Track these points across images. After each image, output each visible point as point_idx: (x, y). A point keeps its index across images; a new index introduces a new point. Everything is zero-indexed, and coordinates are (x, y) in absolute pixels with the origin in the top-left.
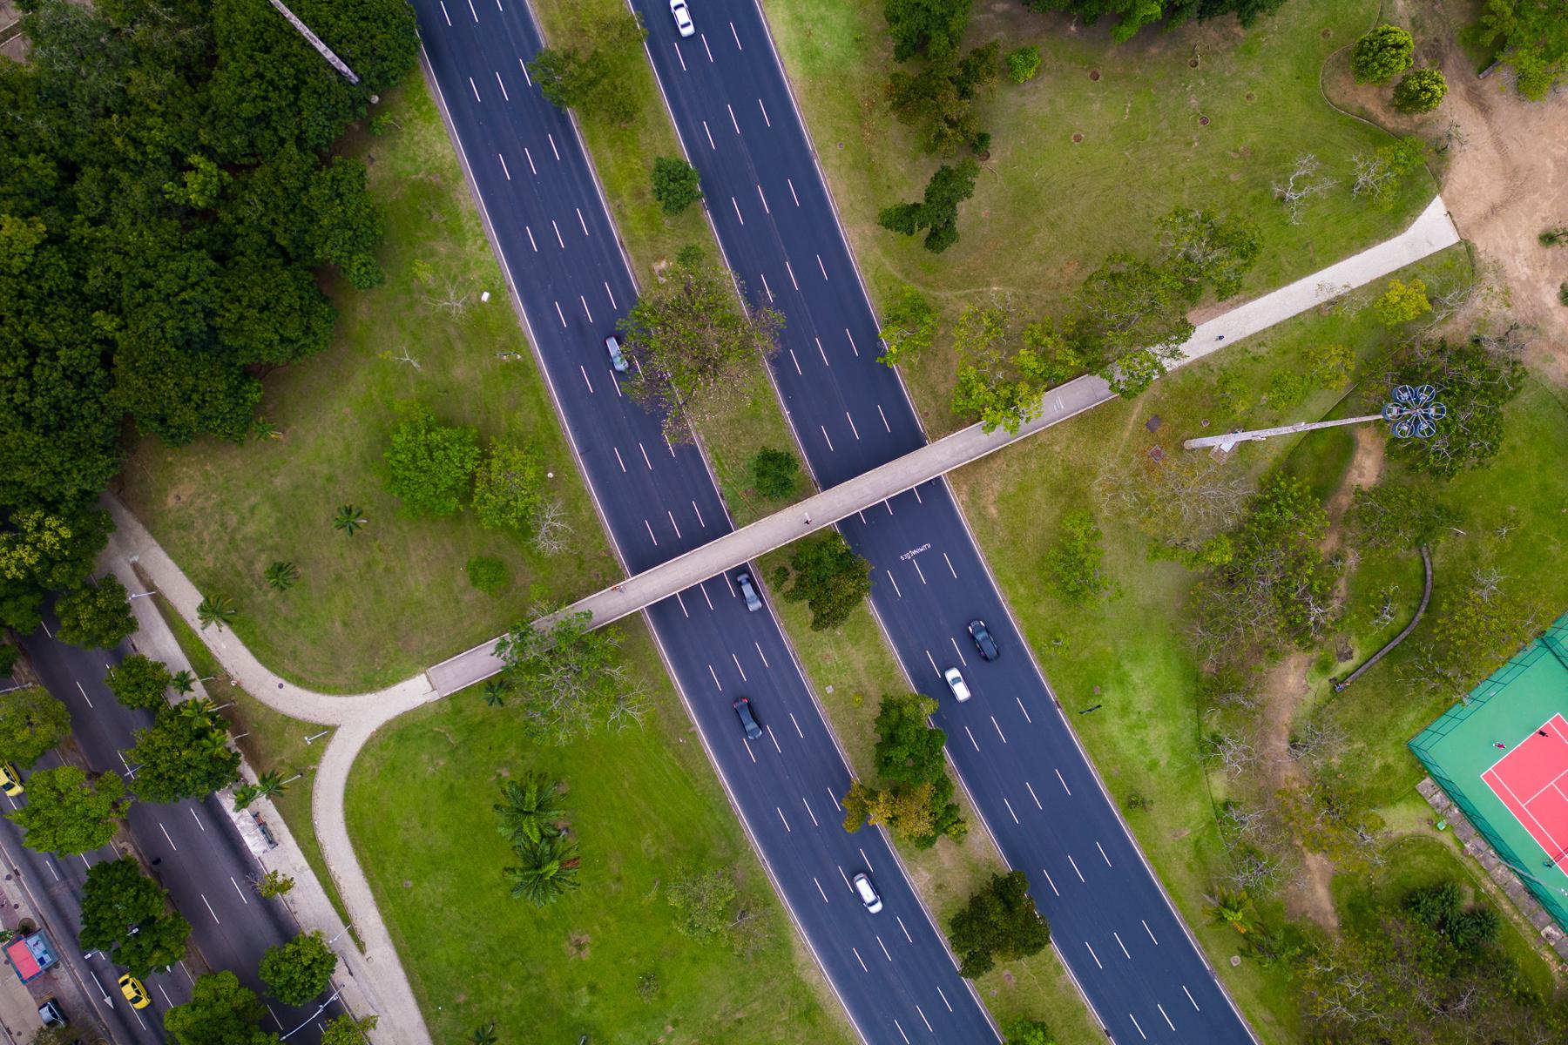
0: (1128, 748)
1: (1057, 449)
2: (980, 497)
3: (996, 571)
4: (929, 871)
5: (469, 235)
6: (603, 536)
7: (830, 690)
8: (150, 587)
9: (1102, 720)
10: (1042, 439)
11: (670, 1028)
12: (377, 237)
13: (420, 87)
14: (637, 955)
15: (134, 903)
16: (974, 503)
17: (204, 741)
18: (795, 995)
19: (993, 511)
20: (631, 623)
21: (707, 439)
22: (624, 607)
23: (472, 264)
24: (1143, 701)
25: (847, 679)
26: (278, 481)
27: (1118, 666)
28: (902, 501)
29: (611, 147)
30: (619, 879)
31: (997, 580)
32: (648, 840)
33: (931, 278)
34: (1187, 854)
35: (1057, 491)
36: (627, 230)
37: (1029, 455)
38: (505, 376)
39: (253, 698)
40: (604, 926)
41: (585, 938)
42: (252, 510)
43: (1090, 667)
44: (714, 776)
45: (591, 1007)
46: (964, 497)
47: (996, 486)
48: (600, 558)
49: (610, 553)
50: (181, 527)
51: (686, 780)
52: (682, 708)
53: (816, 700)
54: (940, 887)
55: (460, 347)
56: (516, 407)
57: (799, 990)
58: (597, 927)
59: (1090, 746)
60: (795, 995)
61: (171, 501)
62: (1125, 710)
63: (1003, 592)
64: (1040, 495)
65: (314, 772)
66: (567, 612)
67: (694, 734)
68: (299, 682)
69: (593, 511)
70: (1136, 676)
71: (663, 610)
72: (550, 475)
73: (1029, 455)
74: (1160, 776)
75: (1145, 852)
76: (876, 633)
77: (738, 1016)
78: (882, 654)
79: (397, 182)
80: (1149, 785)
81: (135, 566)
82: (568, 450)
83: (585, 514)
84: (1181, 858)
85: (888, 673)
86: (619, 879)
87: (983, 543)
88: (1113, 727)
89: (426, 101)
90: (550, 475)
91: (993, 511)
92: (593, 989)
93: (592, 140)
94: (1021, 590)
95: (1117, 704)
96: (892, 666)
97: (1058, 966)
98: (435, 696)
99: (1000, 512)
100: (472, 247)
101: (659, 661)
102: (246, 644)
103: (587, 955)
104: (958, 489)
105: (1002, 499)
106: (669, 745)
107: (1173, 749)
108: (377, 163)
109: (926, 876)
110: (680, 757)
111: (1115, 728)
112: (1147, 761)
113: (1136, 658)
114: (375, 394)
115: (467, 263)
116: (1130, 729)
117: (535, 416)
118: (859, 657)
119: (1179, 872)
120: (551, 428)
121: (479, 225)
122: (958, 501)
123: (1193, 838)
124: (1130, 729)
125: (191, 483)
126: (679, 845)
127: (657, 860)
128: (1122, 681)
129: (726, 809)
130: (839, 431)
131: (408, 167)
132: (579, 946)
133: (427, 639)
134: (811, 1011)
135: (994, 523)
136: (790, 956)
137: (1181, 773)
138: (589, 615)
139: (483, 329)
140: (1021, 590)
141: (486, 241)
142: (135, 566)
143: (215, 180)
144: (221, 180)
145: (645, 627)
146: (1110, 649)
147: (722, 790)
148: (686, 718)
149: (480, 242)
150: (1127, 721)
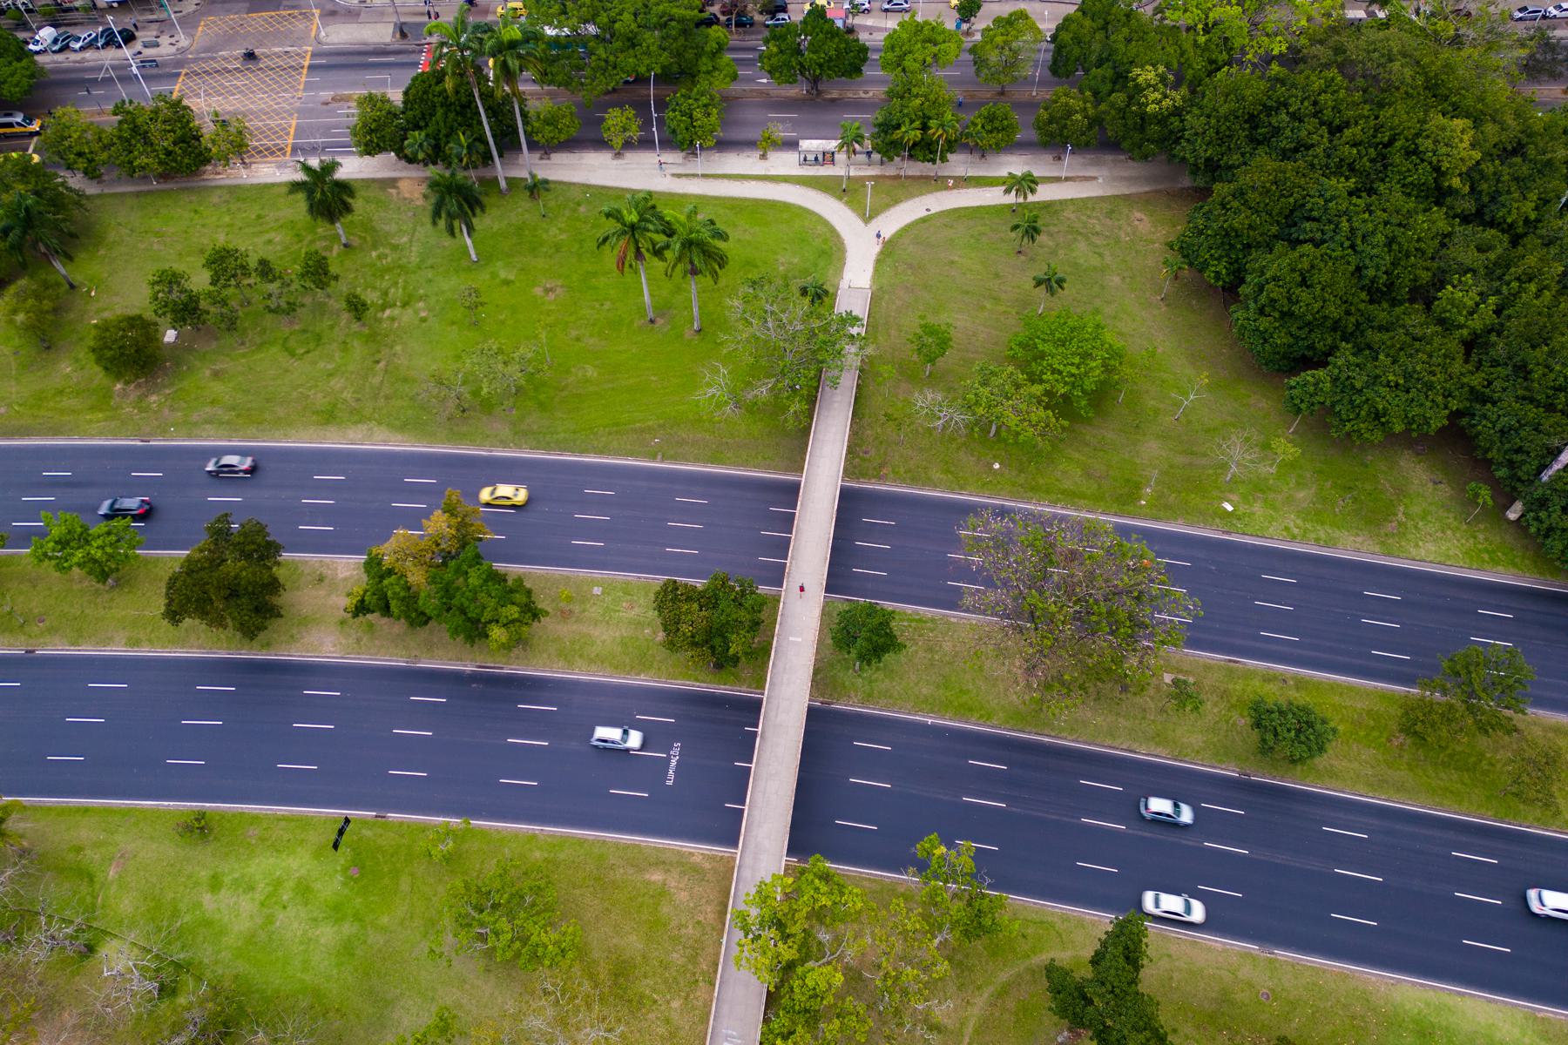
0: (262, 866)
1: (675, 1004)
2: (683, 873)
3: (582, 842)
4: (345, 579)
5: (1309, 526)
6: (903, 480)
7: (597, 590)
8: (1067, 179)
9: (317, 854)
10: (701, 993)
11: (423, 314)
12: (1341, 429)
13: (1514, 565)
14: (503, 322)
15: (823, 66)
16: (680, 864)
17: (917, 124)
18: (353, 411)
19: (657, 877)
20: (797, 442)
21: (948, 623)
22: (820, 436)
23: (1270, 498)
24: (292, 922)
25: (594, 611)
26: (1117, 279)
27: (358, 918)
28: (739, 785)
29: (1369, 712)
30: (578, 339)
31: (573, 837)
32: (591, 372)
33: (1011, 1004)
34: (92, 856)
35: (622, 971)
36: (1249, 674)
37: (693, 959)
38: (1128, 481)
39: (931, 192)
40: (549, 313)
41: (552, 296)
42: (1100, 255)
43: (386, 881)
44: (600, 452)
45: (494, 276)
46: (697, 859)
47: (684, 896)
48: (882, 466)
49: (882, 479)
50: (1112, 211)
51: (617, 424)
52: (684, 459)
53: (597, 574)
54: (321, 579)
55: (1180, 460)
56: (1088, 474)
57: (357, 416)
58: (553, 307)
59: (305, 822)
60: (353, 411)
61: (1138, 215)
62: (304, 890)
63: (553, 835)
64: (633, 943)
65: (840, 199)
66: (848, 382)
67: (653, 458)
68: (923, 220)
69: (935, 486)
70: (327, 934)
71: (791, 492)
72: (997, 466)
73: (693, 959)
74: (197, 884)
75: (143, 811)
76: (618, 667)
77: (382, 364)
78: (591, 661)
79: (1401, 492)
80: (203, 864)
81: (1095, 178)
82: (1013, 497)
83: (936, 475)
84: (97, 845)
86: (578, 339)
87: (627, 847)
88: (299, 863)
89: (1495, 562)
90: (997, 466)
91: (657, 877)
92: (507, 283)
93: (1383, 696)
94: (538, 854)
95: (318, 886)
96: (570, 664)
97: (136, 643)
98: (844, 284)
99: (649, 883)
100: (1293, 521)
101: (745, 464)
102: (979, 207)
103: (538, 291)
104: (713, 858)
105: (662, 893)
106: (660, 426)
107: (208, 923)
108: (1430, 485)
109: (342, 573)
110: (642, 431)
111: (295, 866)
112: (227, 880)
113: (347, 949)
114: (1165, 376)
115: (1275, 508)
116: (278, 884)
117: (1067, 484)
118: (605, 637)
119: (85, 832)
120: (1048, 492)
121: (1317, 540)
122: (698, 850)
123: (99, 877)
124: (278, 884)
125: (1151, 232)
126: (565, 393)
127: (568, 372)
128: (337, 912)
129: (562, 447)
130: (872, 765)
131: (1415, 510)
132: (548, 291)
133: (898, 303)
134: (329, 417)
135: (641, 870)
136: (390, 426)
137: (175, 914)
138: (835, 385)
139: (1193, 482)
140: (538, 854)
141: (1294, 537)
142: (1095, 178)
143: (1462, 320)
144: (1461, 327)
145: (787, 470)
146: (385, 920)
147: (582, 452)
149: (1296, 531)
150: (291, 884)
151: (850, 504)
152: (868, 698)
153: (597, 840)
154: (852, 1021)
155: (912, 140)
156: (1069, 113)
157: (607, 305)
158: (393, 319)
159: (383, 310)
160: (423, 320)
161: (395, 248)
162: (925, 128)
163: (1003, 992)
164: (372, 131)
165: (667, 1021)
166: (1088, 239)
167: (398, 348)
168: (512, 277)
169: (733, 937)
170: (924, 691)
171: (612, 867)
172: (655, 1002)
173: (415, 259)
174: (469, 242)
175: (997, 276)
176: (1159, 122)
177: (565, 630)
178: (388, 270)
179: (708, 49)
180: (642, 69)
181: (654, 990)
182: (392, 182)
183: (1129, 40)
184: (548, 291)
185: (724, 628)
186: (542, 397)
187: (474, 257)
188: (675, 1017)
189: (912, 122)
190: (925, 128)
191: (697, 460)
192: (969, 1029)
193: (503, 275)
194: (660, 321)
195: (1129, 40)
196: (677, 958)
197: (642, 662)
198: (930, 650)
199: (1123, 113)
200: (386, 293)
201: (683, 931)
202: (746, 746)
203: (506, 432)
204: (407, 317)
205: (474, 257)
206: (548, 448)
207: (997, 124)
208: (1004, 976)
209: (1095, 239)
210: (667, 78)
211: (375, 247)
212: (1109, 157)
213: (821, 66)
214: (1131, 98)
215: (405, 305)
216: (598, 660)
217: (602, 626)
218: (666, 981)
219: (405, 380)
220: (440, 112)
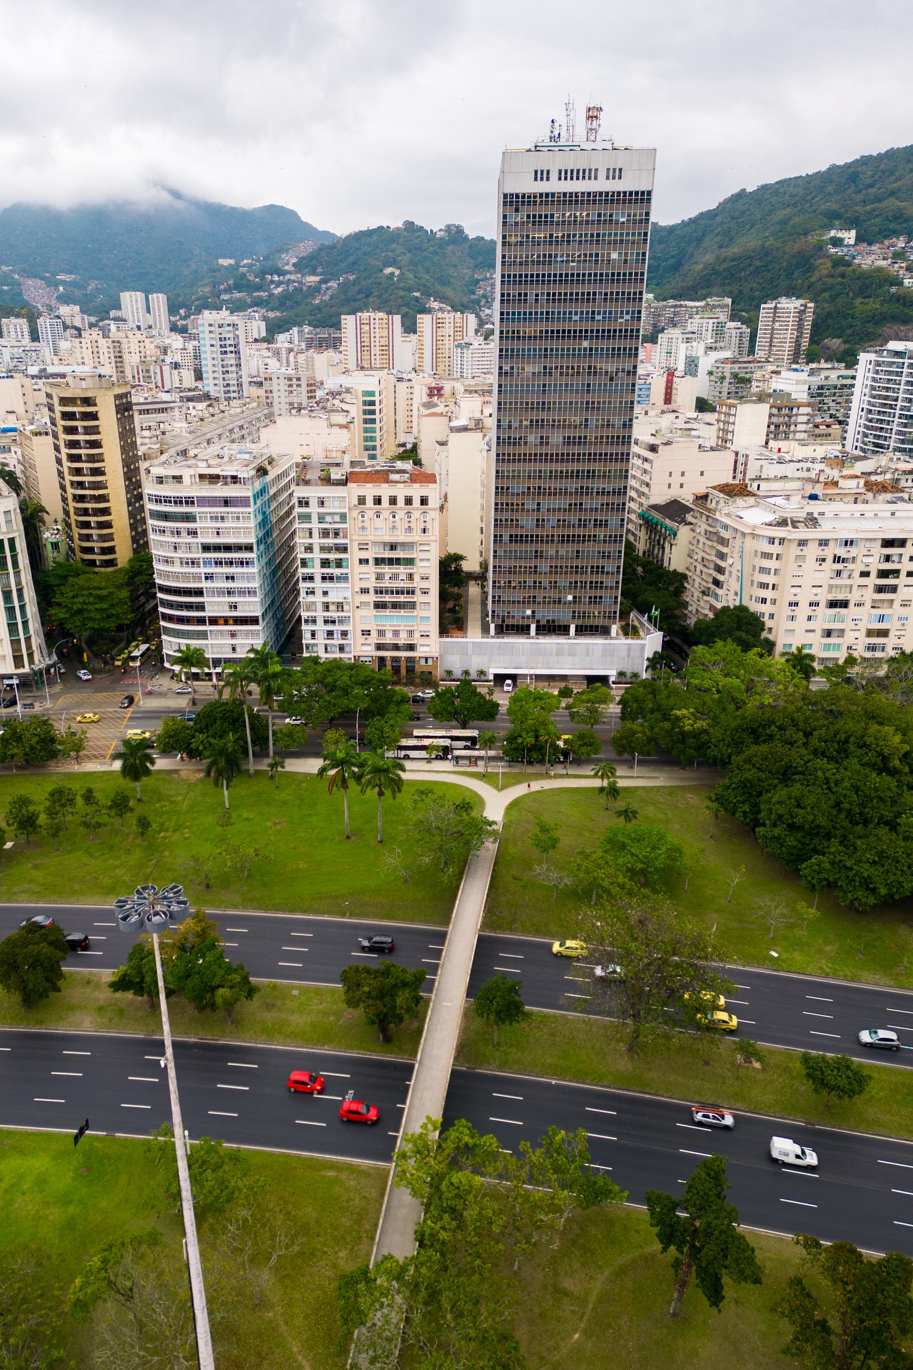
7: (295, 992)
48: (514, 921)
49: (513, 931)
67: (343, 915)
76: (308, 1042)
85: (269, 1033)
101: (411, 920)
113: (70, 1224)
116: (21, 1177)
124: (21, 1177)
146: (104, 1204)
148: (359, 916)
152: (503, 1066)
153: (283, 1154)
155: (529, 751)
156: (634, 733)
157: (316, 831)
158: (165, 838)
159: (159, 832)
160: (187, 838)
161: (173, 802)
162: (537, 737)
164: (170, 737)
165: (335, 1266)
167: (167, 853)
168: (251, 817)
170: (549, 1061)
171: (294, 1168)
172: (325, 1253)
173: (185, 807)
174: (226, 792)
175: (592, 820)
176: (694, 737)
177: (270, 1017)
178: (166, 813)
179: (395, 699)
180: (352, 706)
181: (325, 1245)
182: (176, 771)
183: (668, 697)
184: (276, 824)
185: (391, 1002)
186: (266, 879)
187: (227, 805)
188: (342, 1263)
189: (528, 733)
190: (537, 737)
191: (375, 916)
193: (245, 815)
194: (353, 838)
195: (668, 697)
196: (345, 1221)
197: (326, 1038)
198: (553, 1034)
199: (669, 733)
200: (163, 824)
201: (351, 1203)
203: (237, 899)
204: (177, 836)
205: (227, 805)
206: (266, 909)
207: (586, 741)
209: (661, 806)
210: (367, 714)
211: (159, 801)
212: (667, 768)
213: (468, 710)
214: (673, 725)
215: (175, 831)
216: (293, 1036)
218: (334, 1238)
219: (169, 870)
220: (219, 722)
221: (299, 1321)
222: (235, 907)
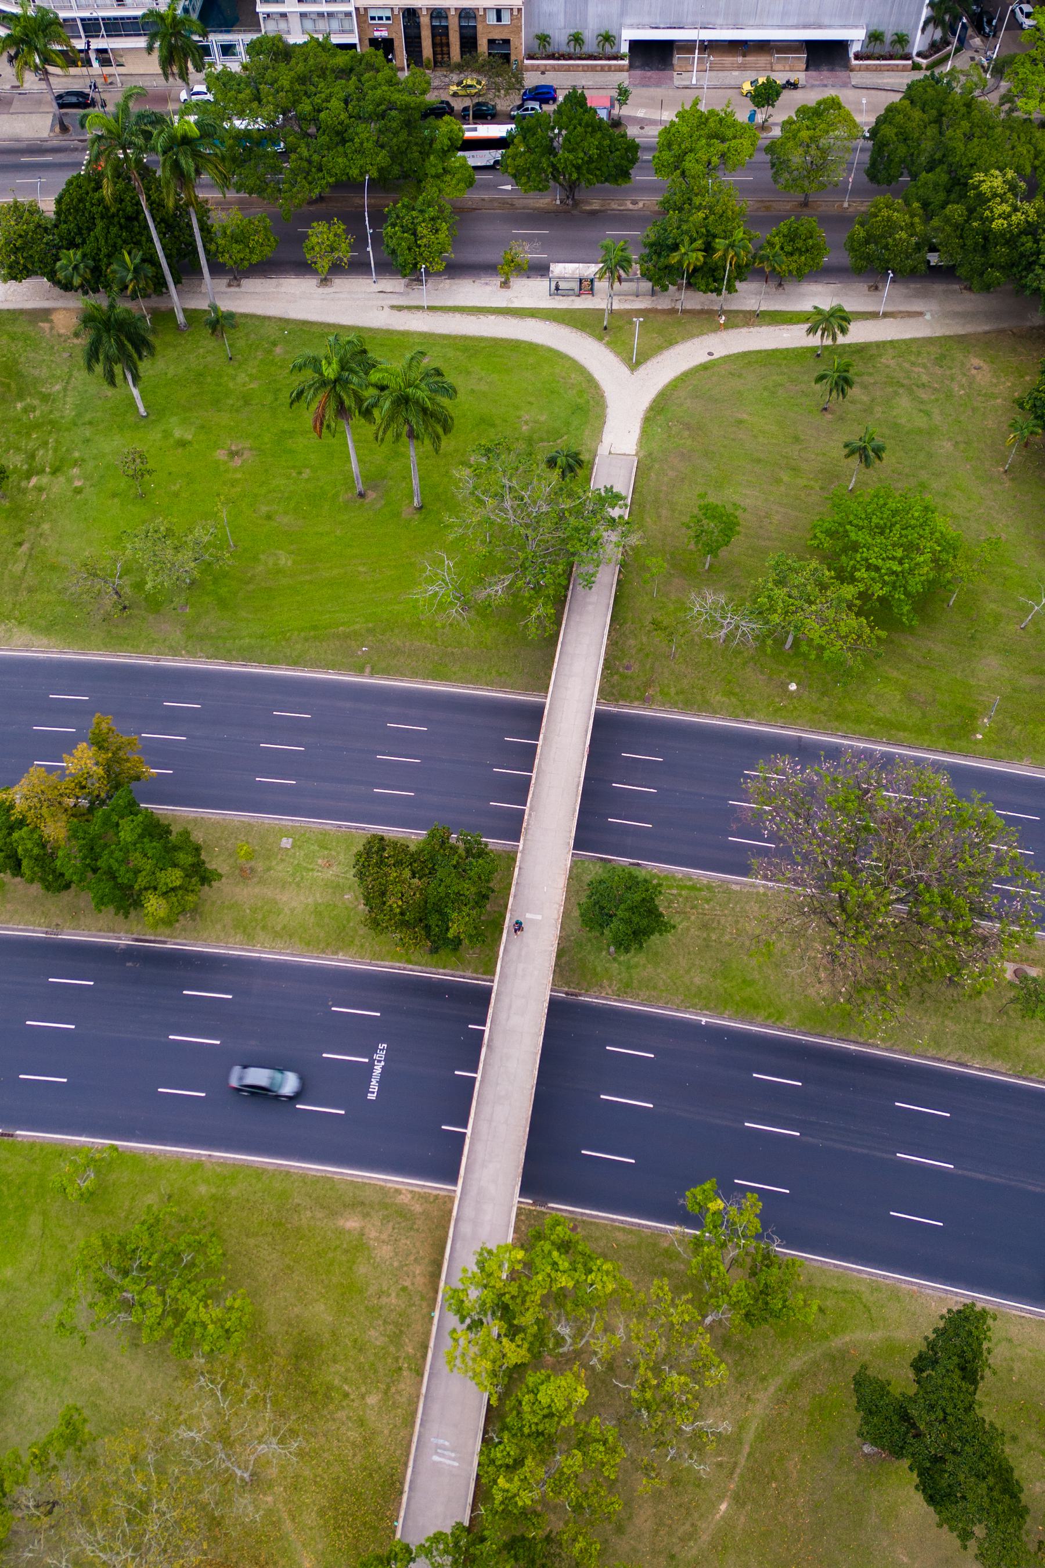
1: (372, 1400)
2: (386, 1219)
3: (260, 1173)
6: (674, 704)
7: (286, 843)
8: (886, 315)
10: (405, 1385)
11: (78, 484)
14: (176, 495)
16: (385, 1206)
17: (699, 243)
19: (352, 1223)
20: (540, 655)
21: (728, 891)
22: (569, 649)
25: (281, 870)
26: (948, 446)
28: (459, 1101)
30: (269, 517)
31: (248, 1166)
32: (285, 560)
33: (804, 1400)
35: (305, 1352)
37: (396, 1339)
38: (960, 708)
40: (233, 483)
41: (238, 461)
42: (928, 414)
44: (295, 662)
45: (167, 434)
46: (405, 1199)
47: (385, 1252)
48: (648, 684)
49: (646, 701)
50: (943, 357)
51: (315, 628)
53: (287, 821)
56: (909, 699)
58: (239, 476)
61: (976, 362)
63: (224, 1164)
64: (320, 1314)
65: (600, 339)
66: (607, 579)
67: (360, 670)
68: (704, 367)
72: (793, 687)
73: (396, 1339)
76: (311, 944)
77: (26, 547)
78: (277, 935)
81: (921, 314)
82: (815, 727)
83: (716, 697)
85: (245, 928)
86: (269, 517)
90: (793, 687)
91: (352, 1223)
92: (182, 444)
94: (203, 1189)
98: (603, 450)
99: (341, 1232)
101: (475, 680)
102: (775, 351)
103: (220, 455)
104: (424, 1198)
105: (359, 1246)
106: (369, 630)
110: (347, 636)
114: (1009, 571)
117: (882, 712)
118: (295, 903)
120: (858, 721)
126: (251, 587)
127: (255, 559)
129: (248, 655)
132: (233, 454)
135: (333, 1214)
138: (589, 584)
140: (203, 1189)
142: (921, 314)
145: (526, 689)
147: (272, 662)
148: (386, 672)
151: (608, 734)
152: (626, 989)
153: (279, 1171)
154: (598, 1452)
156: (891, 227)
157: (307, 473)
158: (40, 489)
159: (28, 478)
160: (78, 491)
161: (45, 398)
162: (708, 249)
163: (795, 1384)
164: (16, 250)
165: (361, 1422)
166: (910, 391)
167: (46, 527)
168: (189, 437)
169: (444, 1319)
170: (697, 981)
171: (296, 1209)
172: (346, 1395)
173: (69, 412)
174: (135, 392)
175: (797, 439)
176: (1007, 242)
177: (246, 894)
178: (37, 426)
179: (437, 146)
180: (355, 172)
181: (345, 1380)
182: (44, 314)
183: (969, 137)
184: (233, 454)
185: (443, 897)
186: (223, 591)
187: (142, 410)
188: (371, 1416)
189: (693, 240)
190: (708, 249)
191: (414, 674)
192: (750, 1436)
193: (178, 433)
194: (372, 495)
195: (969, 137)
196: (376, 1337)
197: (341, 939)
198: (705, 926)
199: (960, 229)
200: (32, 456)
201: (384, 1300)
202: (470, 1050)
203: (176, 636)
204: (58, 486)
205: (142, 410)
206: (229, 656)
207: (799, 244)
208: (796, 1363)
209: (922, 394)
211: (20, 396)
213: (578, 168)
214: (971, 211)
215: (55, 472)
216: (286, 934)
217: (289, 890)
218: (360, 1369)
219: (53, 568)
220: (100, 224)
221: (310, 1518)
222: (174, 651)
